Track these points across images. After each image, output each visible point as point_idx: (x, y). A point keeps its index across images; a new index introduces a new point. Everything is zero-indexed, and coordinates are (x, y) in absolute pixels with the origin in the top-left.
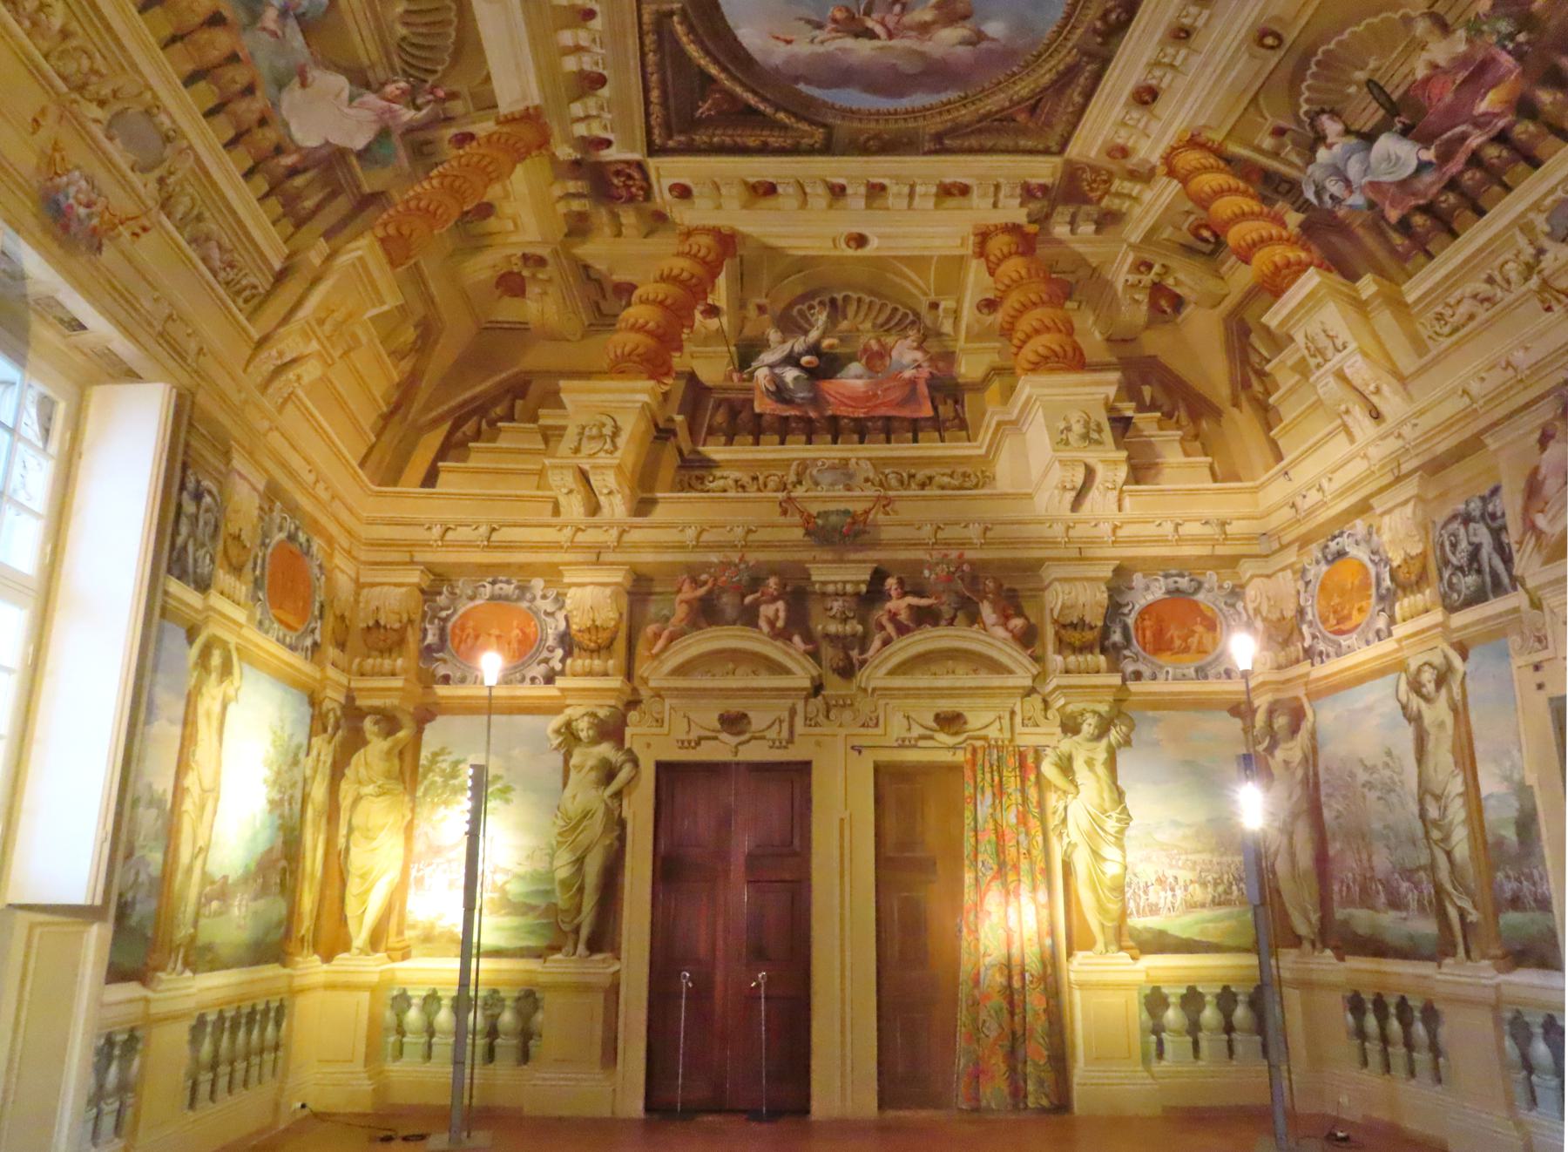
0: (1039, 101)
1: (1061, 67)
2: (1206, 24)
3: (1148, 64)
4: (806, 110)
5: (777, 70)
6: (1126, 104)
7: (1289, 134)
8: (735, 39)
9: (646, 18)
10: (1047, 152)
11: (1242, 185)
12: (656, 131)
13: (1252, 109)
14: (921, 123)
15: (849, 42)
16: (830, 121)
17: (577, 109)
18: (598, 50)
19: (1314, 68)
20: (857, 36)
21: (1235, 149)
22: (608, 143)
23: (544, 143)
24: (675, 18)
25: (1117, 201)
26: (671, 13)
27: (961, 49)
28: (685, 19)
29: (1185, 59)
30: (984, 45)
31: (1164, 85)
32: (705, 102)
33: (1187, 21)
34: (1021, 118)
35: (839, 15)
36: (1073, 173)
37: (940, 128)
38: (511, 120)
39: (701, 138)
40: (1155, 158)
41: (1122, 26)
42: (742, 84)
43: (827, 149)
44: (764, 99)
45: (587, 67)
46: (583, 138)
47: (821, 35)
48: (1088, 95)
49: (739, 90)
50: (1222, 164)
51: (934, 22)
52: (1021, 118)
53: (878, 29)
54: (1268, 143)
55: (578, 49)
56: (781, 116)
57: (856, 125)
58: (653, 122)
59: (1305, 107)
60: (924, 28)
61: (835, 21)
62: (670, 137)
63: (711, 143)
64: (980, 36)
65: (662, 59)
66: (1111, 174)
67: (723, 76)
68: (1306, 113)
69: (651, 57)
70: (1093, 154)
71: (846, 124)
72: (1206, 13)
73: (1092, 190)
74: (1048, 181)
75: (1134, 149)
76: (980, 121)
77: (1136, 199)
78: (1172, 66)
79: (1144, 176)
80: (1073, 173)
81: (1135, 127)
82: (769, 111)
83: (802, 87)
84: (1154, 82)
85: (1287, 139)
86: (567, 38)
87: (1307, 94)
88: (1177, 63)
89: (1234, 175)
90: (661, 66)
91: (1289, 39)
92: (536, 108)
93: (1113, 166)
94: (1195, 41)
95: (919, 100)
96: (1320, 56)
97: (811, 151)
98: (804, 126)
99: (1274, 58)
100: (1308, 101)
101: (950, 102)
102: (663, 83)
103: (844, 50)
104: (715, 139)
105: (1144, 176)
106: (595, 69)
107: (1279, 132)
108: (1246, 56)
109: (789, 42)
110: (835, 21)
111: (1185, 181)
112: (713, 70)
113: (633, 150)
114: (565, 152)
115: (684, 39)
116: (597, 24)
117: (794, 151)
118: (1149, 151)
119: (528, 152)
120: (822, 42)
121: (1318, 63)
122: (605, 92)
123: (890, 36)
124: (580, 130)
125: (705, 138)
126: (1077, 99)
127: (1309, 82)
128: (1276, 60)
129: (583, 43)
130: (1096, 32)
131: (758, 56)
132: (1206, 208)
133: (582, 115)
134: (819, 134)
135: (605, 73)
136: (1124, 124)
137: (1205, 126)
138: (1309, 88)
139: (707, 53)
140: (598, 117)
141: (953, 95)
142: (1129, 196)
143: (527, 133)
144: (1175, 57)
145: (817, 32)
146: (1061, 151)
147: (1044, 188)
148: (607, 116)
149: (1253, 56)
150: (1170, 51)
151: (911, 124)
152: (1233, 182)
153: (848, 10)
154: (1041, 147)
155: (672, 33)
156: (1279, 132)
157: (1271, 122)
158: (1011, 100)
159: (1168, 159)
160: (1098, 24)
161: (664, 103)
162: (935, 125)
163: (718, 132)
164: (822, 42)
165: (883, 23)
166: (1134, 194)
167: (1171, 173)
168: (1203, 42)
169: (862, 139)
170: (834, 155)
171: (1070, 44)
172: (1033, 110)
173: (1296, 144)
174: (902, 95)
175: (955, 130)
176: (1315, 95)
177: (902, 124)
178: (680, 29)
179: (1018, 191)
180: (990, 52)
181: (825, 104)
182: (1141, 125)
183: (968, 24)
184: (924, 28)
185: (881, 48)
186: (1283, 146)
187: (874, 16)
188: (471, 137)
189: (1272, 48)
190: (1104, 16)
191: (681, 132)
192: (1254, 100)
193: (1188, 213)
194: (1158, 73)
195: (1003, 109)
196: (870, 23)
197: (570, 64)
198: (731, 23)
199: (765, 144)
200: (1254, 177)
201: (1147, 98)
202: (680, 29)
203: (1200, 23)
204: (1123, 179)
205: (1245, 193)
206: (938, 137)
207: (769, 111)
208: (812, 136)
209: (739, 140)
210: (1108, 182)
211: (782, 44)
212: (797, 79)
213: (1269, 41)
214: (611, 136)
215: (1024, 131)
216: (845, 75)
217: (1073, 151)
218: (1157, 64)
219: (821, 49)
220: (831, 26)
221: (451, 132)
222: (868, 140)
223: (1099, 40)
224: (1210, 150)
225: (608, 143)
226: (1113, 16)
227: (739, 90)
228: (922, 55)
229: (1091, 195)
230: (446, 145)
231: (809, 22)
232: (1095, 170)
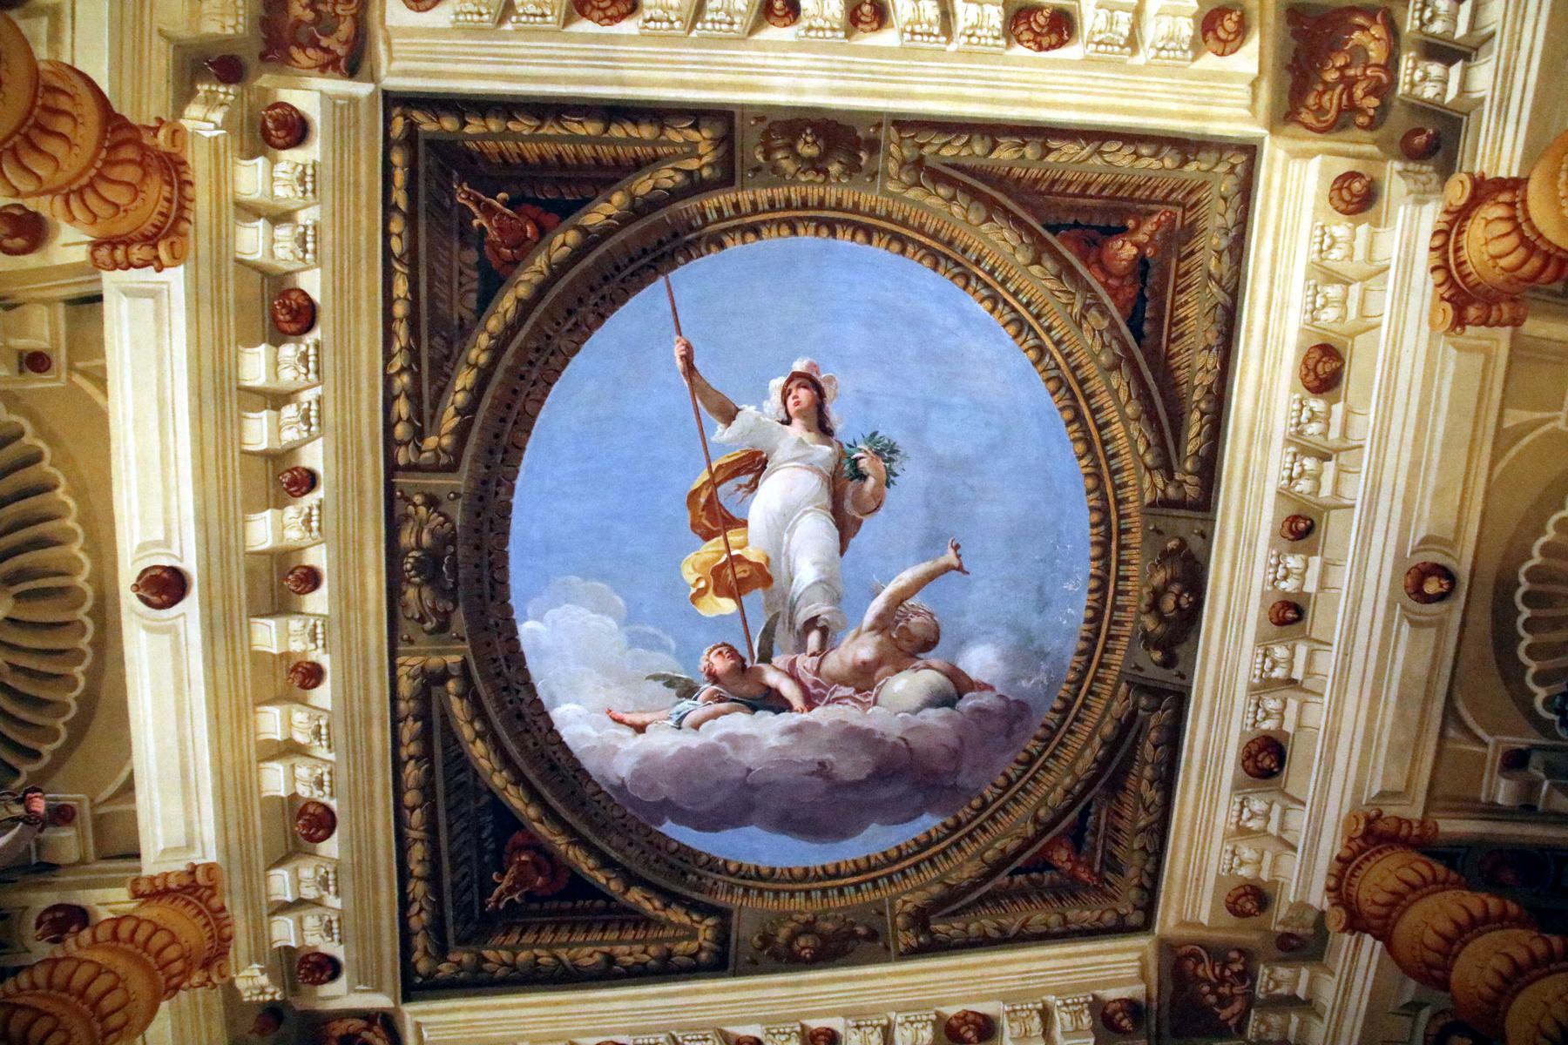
0: (1085, 814)
1: (1108, 729)
2: (1322, 586)
3: (1252, 689)
4: (682, 877)
5: (621, 788)
6: (1237, 787)
7: (1536, 758)
8: (550, 723)
9: (405, 687)
10: (1122, 929)
11: (1493, 903)
12: (419, 942)
13: (1452, 733)
14: (886, 891)
15: (740, 722)
16: (722, 899)
17: (281, 883)
18: (322, 752)
19: (1526, 613)
20: (753, 707)
21: (1453, 827)
22: (327, 968)
23: (216, 954)
24: (451, 685)
25: (1274, 1020)
26: (443, 676)
27: (933, 716)
28: (468, 691)
29: (1310, 661)
30: (969, 701)
31: (1289, 727)
32: (503, 874)
33: (1289, 586)
34: (1061, 856)
35: (721, 665)
36: (1178, 962)
37: (919, 898)
38: (158, 892)
39: (496, 955)
40: (1318, 898)
41: (1188, 621)
42: (567, 829)
43: (720, 964)
44: (606, 863)
45: (304, 791)
46: (288, 950)
47: (696, 708)
48: (1167, 781)
49: (561, 843)
50: (1440, 869)
51: (879, 662)
52: (1061, 856)
53: (788, 689)
54: (1504, 791)
55: (289, 750)
56: (635, 895)
57: (770, 903)
58: (415, 923)
59: (1541, 694)
60: (864, 678)
61: (713, 677)
62: (442, 953)
63: (513, 966)
64: (959, 684)
65: (430, 772)
66: (1246, 953)
67: (532, 812)
68: (1548, 702)
69: (412, 772)
70: (1204, 917)
71: (754, 902)
72: (1315, 562)
73: (1223, 1001)
74: (1136, 991)
75: (1274, 883)
76: (987, 877)
77: (1306, 1005)
78: (1290, 682)
79: (1303, 946)
80: (1178, 962)
81: (1263, 832)
82: (615, 886)
83: (672, 830)
84: (1269, 725)
85: (1536, 770)
86: (272, 722)
87: (1533, 667)
88: (1298, 674)
89: (1471, 887)
90: (427, 788)
91: (1463, 569)
92: (209, 868)
93: (1247, 934)
94: (1318, 621)
95: (877, 839)
96: (1525, 586)
97: (693, 969)
98: (677, 915)
99: (1453, 612)
100: (1541, 678)
101: (930, 843)
102: (431, 827)
103: (732, 739)
104: (523, 956)
105: (1303, 946)
106: (317, 795)
107: (1515, 761)
108: (1405, 628)
109: (640, 729)
110: (713, 677)
111: (1384, 934)
112: (515, 799)
113: (378, 989)
114: (254, 981)
115: (467, 732)
116: (323, 696)
117: (666, 970)
118: (1303, 883)
119: (186, 974)
120: (696, 726)
121: (1527, 599)
122: (331, 847)
123: (810, 702)
124: (284, 931)
125: (505, 955)
126: (1152, 795)
127: (1528, 639)
128: (1456, 618)
129: (301, 738)
130: (1149, 641)
131: (590, 764)
132: (1444, 985)
133: (289, 898)
134: (706, 930)
135: (333, 804)
136: (1242, 831)
137: (1382, 795)
138: (1530, 651)
139: (507, 761)
140: (317, 903)
141: (929, 822)
142: (1291, 1002)
143: (187, 927)
144: (1291, 662)
145: (686, 704)
146: (1146, 926)
147: (1132, 1007)
148: (334, 902)
149: (1413, 623)
150: (1280, 652)
151: (869, 895)
152: (1474, 902)
153: (733, 653)
154: (1109, 917)
155: (446, 716)
156: (1515, 761)
157: (1494, 746)
158: (1036, 820)
159: (1340, 888)
160: (1149, 623)
161: (434, 879)
162: (909, 895)
163: (529, 939)
164: (696, 726)
165: (792, 674)
166: (1301, 992)
167: (1356, 923)
168: (1330, 619)
169: (784, 933)
170: (736, 974)
171: (1111, 676)
172: (1077, 836)
173: (1550, 771)
174: (842, 834)
175: (950, 901)
176: (1549, 664)
177: (852, 898)
178: (458, 708)
179: (1086, 1020)
180: (979, 711)
181: (711, 864)
182: (1273, 828)
183: (933, 657)
184: (864, 678)
185: (797, 730)
186: (1534, 786)
187: (779, 660)
188: (79, 916)
189: (1441, 597)
190: (1155, 606)
191: (462, 942)
192: (1450, 710)
193: (1414, 1007)
194: (1272, 704)
195: (1029, 843)
196: (772, 678)
197: (276, 780)
198: (542, 694)
199: (610, 959)
200: (1508, 875)
201: (1267, 762)
202: (458, 708)
203: (1311, 587)
204: (1272, 961)
205: (1503, 920)
206: (920, 919)
207: (615, 886)
208: (693, 935)
209: (563, 954)
210: (1247, 975)
211: (628, 732)
212: (668, 808)
213: (1432, 586)
214: (337, 951)
215: (1068, 890)
216: (740, 798)
217: (1168, 920)
218: (1264, 686)
219: (693, 741)
220: (707, 688)
221: (49, 898)
222: (794, 936)
223: (1157, 656)
224: (1408, 843)
225: (327, 968)
226: (1169, 604)
227: (561, 843)
228: (862, 738)
229: (1224, 1014)
230: (30, 929)
231: (670, 682)
232: (1217, 953)
